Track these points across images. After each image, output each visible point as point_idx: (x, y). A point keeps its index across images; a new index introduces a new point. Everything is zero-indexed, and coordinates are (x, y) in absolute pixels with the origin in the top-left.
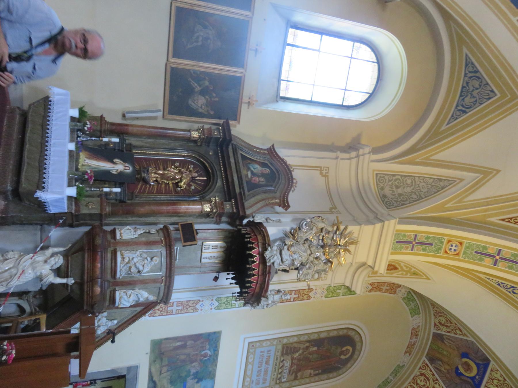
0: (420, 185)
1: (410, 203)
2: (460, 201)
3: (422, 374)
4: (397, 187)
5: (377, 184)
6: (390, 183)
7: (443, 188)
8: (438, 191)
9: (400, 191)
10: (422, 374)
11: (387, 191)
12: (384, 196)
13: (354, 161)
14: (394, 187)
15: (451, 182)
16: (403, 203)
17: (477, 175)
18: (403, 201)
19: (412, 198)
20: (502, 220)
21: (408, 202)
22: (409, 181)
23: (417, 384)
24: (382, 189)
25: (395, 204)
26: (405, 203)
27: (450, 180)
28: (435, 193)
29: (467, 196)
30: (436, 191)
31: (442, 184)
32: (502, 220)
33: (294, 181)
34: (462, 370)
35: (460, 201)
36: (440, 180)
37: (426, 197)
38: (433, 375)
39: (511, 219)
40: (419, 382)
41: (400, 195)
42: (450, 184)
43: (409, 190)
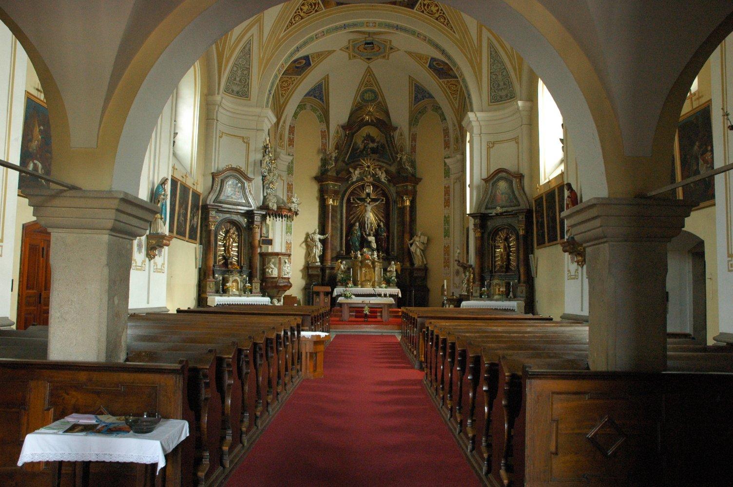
0: (241, 63)
1: (249, 79)
2: (263, 47)
3: (283, 82)
4: (235, 79)
5: (229, 93)
6: (231, 83)
7: (249, 50)
8: (250, 54)
9: (238, 79)
10: (283, 82)
11: (236, 89)
12: (238, 92)
13: (221, 110)
14: (234, 82)
15: (249, 42)
16: (246, 84)
17: (257, 24)
18: (245, 83)
19: (246, 75)
20: (285, 31)
21: (247, 80)
22: (235, 69)
23: (284, 87)
24: (233, 91)
25: (246, 90)
26: (247, 82)
27: (248, 42)
28: (250, 57)
29: (263, 42)
30: (248, 56)
31: (247, 48)
32: (285, 31)
33: (238, 168)
34: (297, 66)
35: (263, 47)
36: (244, 48)
37: (249, 65)
38: (288, 77)
39: (287, 26)
40: (284, 85)
41: (240, 81)
42: (250, 44)
43: (239, 72)
